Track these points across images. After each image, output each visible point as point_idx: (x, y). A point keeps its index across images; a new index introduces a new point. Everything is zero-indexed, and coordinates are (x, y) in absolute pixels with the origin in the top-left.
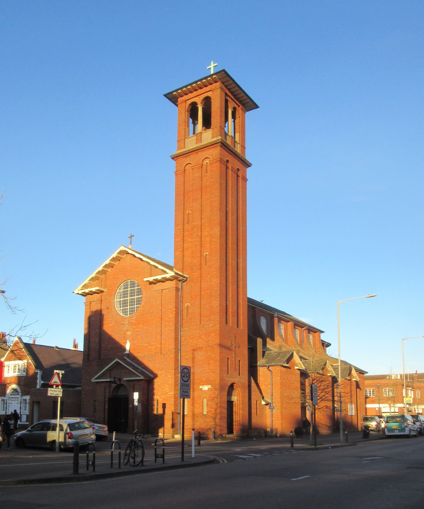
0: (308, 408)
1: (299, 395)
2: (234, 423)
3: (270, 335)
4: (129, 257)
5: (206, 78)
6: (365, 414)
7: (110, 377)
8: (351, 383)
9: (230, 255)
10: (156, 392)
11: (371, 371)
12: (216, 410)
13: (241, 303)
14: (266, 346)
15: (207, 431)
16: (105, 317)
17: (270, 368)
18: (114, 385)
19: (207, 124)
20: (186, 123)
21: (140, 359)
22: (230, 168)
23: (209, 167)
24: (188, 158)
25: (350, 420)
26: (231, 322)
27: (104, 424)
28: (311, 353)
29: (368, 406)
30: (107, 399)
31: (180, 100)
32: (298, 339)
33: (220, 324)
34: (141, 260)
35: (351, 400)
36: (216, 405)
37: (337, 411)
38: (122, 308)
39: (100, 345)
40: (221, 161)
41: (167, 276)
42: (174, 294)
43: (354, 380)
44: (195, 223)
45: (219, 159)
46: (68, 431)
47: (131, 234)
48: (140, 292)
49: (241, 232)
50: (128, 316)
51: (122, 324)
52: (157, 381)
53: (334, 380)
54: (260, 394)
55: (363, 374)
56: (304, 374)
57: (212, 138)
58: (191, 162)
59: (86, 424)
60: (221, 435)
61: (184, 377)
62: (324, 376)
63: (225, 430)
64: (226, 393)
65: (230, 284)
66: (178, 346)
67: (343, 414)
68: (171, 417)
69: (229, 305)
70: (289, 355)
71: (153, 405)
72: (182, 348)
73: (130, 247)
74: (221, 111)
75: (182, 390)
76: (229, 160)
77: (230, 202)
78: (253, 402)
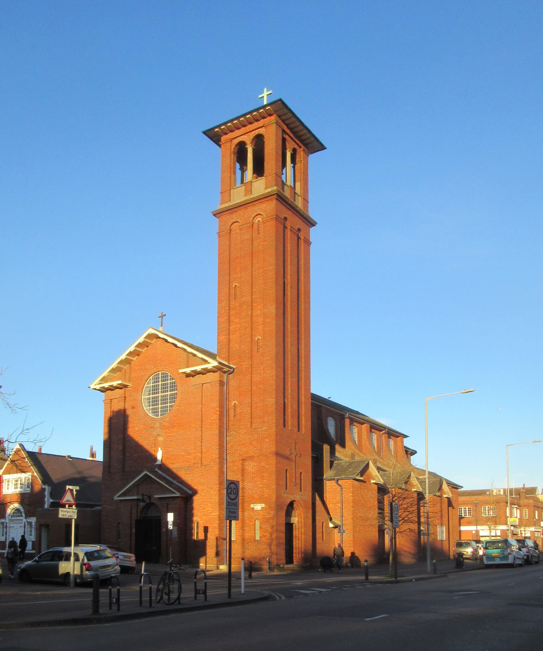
0: (387, 532)
1: (376, 515)
2: (294, 551)
3: (340, 441)
5: (257, 110)
6: (458, 538)
7: (138, 494)
8: (441, 500)
9: (289, 339)
10: (195, 512)
11: (467, 486)
12: (271, 535)
13: (303, 400)
14: (335, 454)
15: (260, 560)
16: (130, 419)
17: (340, 482)
18: (142, 504)
19: (259, 170)
20: (232, 170)
21: (175, 471)
22: (289, 227)
25: (439, 546)
26: (290, 424)
27: (131, 553)
28: (391, 463)
29: (463, 528)
30: (134, 522)
31: (224, 138)
32: (376, 445)
33: (276, 426)
34: (175, 346)
35: (442, 521)
36: (272, 527)
37: (424, 534)
38: (151, 407)
39: (124, 454)
40: (277, 218)
42: (218, 389)
43: (445, 496)
45: (274, 216)
46: (86, 561)
47: (162, 313)
48: (174, 387)
49: (303, 310)
50: (160, 417)
51: (152, 428)
52: (196, 498)
53: (420, 496)
54: (326, 515)
55: (457, 489)
56: (382, 490)
57: (266, 188)
59: (108, 552)
60: (278, 565)
61: (230, 493)
62: (407, 492)
63: (284, 561)
64: (284, 514)
65: (289, 376)
66: (223, 454)
67: (430, 539)
68: (215, 544)
69: (288, 404)
70: (364, 466)
71: (191, 529)
73: (161, 329)
74: (277, 153)
75: (228, 510)
76: (288, 218)
77: (289, 271)
78: (319, 524)
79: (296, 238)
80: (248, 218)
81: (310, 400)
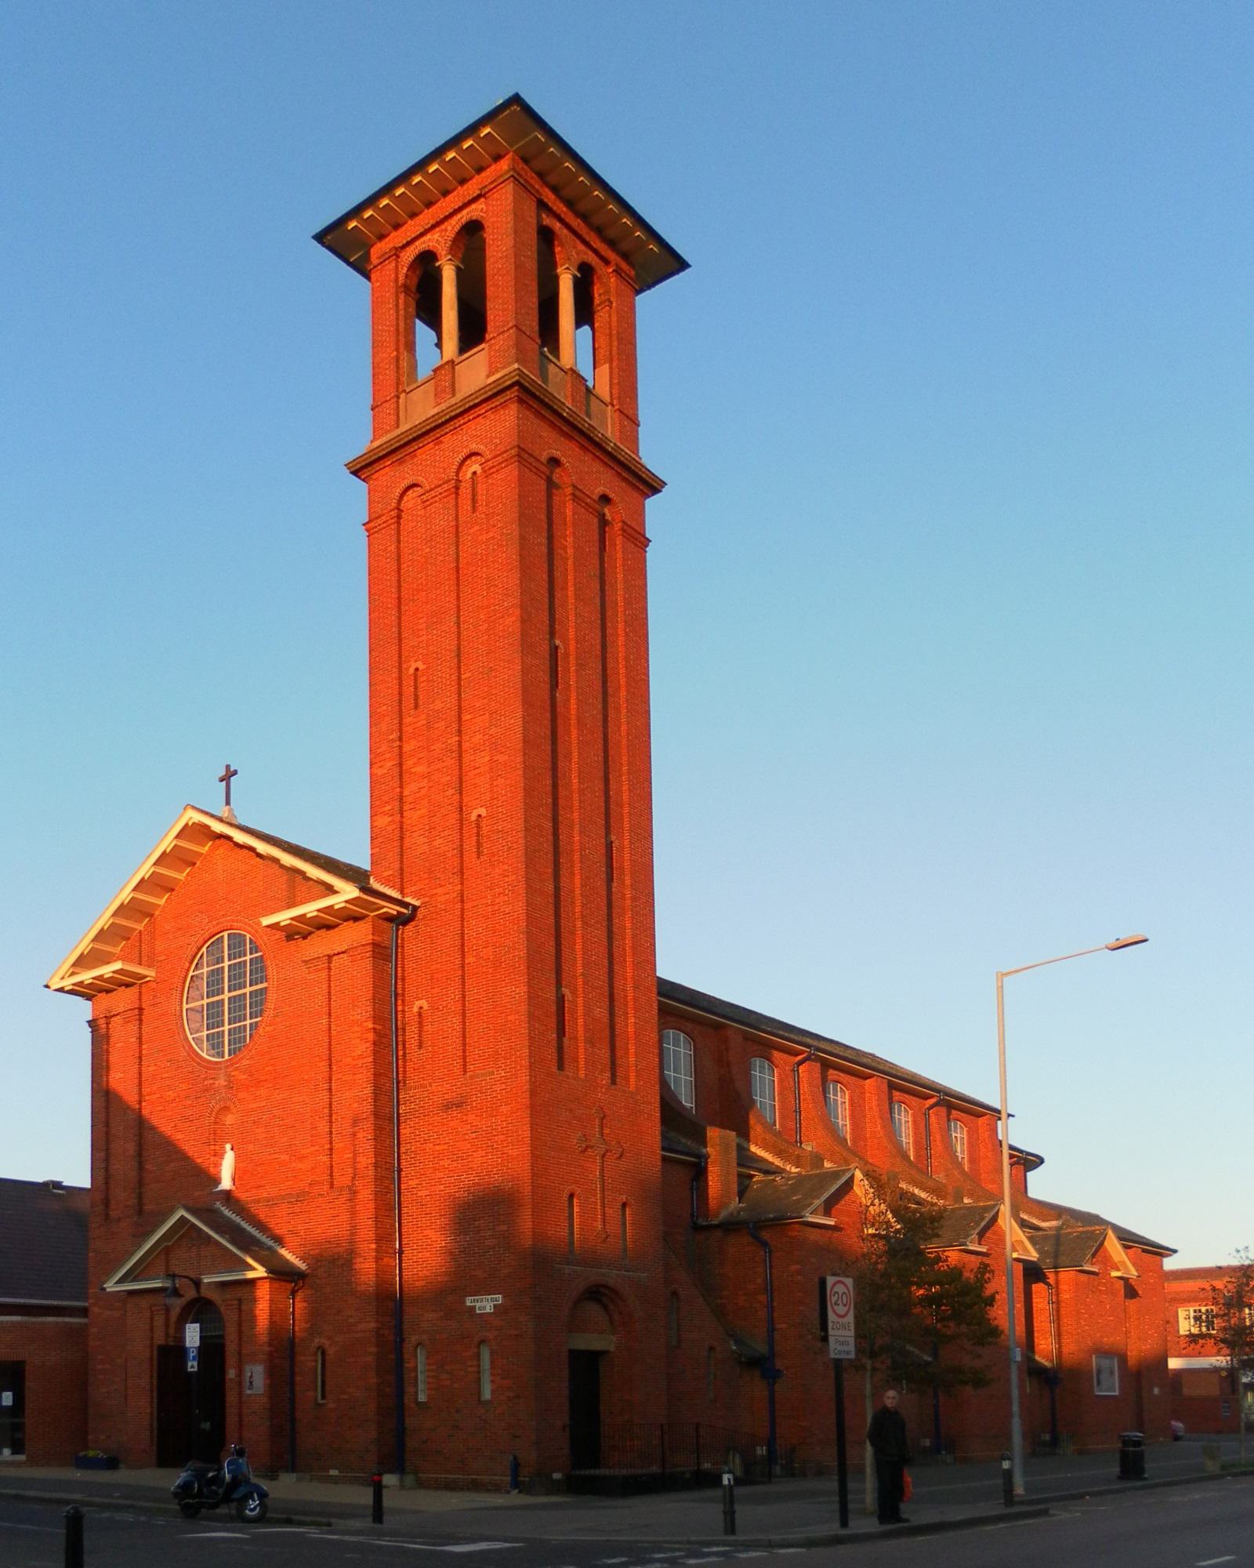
20: (402, 340)
24: (407, 467)
42: (370, 967)
44: (438, 705)
47: (228, 767)
57: (488, 376)
69: (574, 1002)
81: (654, 996)
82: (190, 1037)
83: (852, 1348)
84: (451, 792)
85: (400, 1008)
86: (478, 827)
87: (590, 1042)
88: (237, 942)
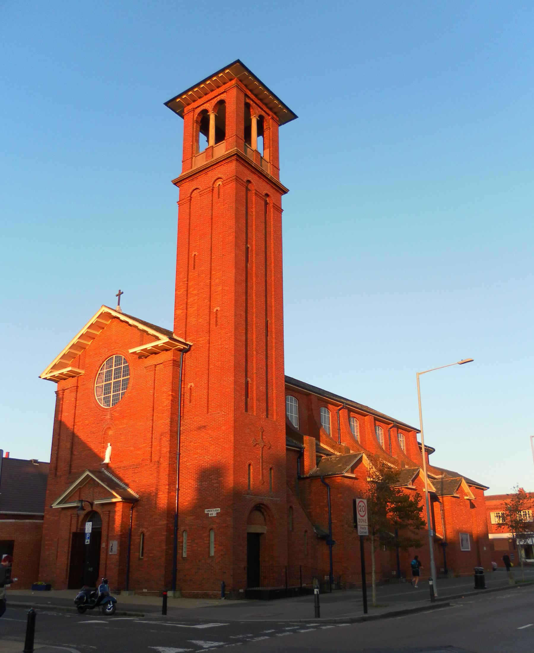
4: (115, 323)
19: (220, 136)
23: (221, 190)
31: (186, 110)
41: (159, 343)
44: (203, 268)
58: (199, 187)
72: (181, 451)
74: (238, 115)
79: (263, 203)
80: (208, 183)
82: (97, 398)
83: (367, 530)
84: (206, 301)
85: (183, 386)
86: (216, 314)
87: (258, 400)
88: (119, 359)
